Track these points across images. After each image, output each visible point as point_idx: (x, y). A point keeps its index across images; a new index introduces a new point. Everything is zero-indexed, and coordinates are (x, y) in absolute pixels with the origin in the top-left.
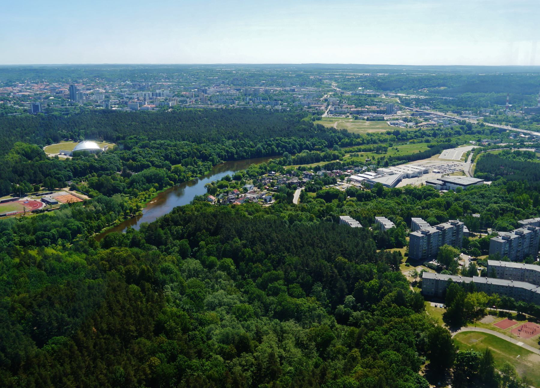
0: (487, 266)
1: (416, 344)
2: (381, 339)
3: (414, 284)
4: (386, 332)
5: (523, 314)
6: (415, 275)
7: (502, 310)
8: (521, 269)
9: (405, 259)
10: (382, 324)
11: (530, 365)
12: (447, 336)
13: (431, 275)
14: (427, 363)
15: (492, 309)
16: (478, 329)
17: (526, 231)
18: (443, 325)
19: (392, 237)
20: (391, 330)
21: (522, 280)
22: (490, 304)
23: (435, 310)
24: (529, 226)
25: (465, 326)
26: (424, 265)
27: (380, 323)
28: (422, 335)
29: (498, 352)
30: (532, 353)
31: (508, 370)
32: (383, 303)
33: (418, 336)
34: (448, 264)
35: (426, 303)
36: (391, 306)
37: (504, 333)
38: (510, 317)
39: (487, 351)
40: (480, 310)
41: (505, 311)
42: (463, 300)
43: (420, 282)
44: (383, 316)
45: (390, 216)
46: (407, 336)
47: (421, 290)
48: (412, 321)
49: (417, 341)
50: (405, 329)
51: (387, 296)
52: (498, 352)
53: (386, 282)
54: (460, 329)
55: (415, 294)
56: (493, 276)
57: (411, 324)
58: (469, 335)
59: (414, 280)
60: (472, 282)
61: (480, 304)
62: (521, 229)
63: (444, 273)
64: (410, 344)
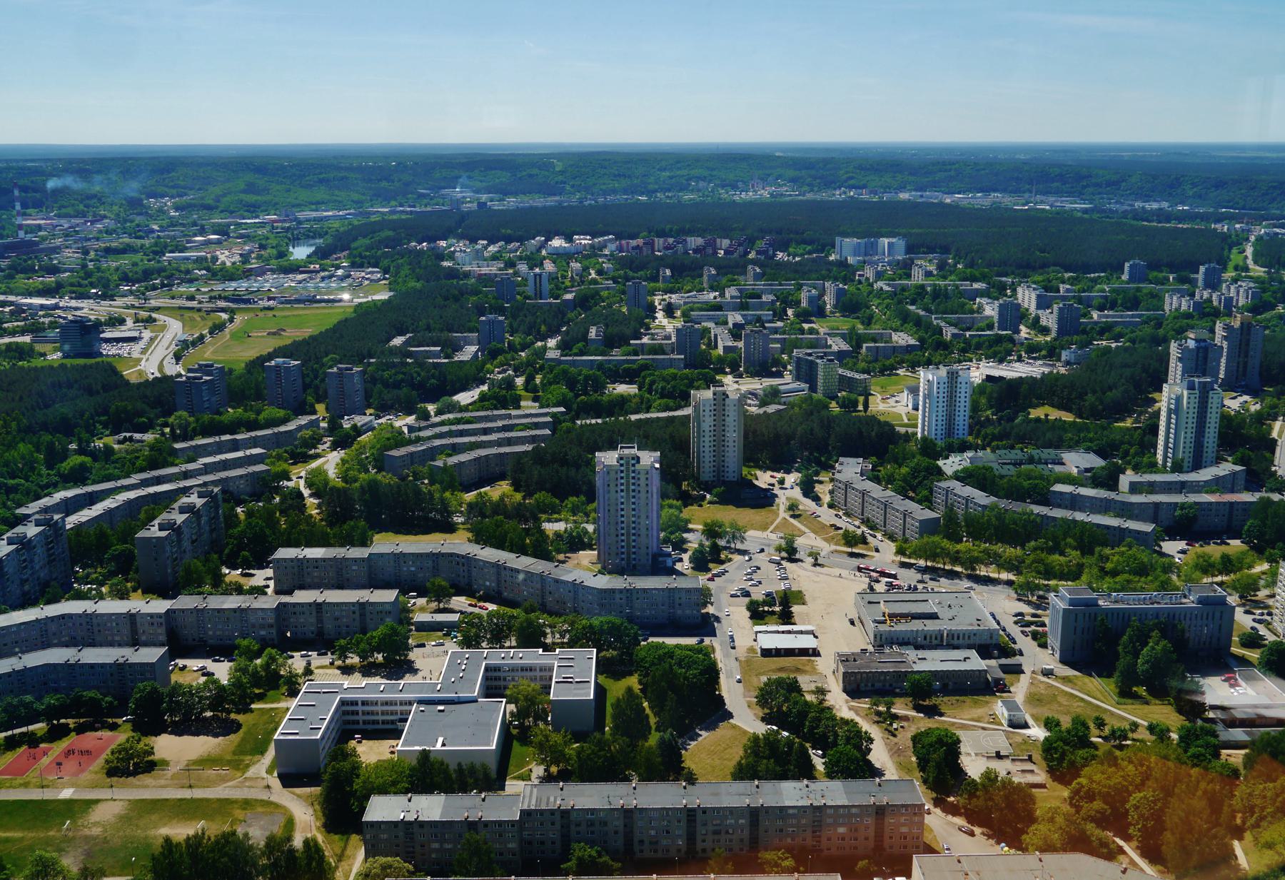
5: (62, 721)
7: (10, 733)
11: (96, 831)
17: (31, 531)
21: (45, 645)
24: (37, 516)
29: (17, 834)
30: (97, 801)
37: (26, 785)
41: (17, 731)
52: (17, 834)
62: (19, 529)
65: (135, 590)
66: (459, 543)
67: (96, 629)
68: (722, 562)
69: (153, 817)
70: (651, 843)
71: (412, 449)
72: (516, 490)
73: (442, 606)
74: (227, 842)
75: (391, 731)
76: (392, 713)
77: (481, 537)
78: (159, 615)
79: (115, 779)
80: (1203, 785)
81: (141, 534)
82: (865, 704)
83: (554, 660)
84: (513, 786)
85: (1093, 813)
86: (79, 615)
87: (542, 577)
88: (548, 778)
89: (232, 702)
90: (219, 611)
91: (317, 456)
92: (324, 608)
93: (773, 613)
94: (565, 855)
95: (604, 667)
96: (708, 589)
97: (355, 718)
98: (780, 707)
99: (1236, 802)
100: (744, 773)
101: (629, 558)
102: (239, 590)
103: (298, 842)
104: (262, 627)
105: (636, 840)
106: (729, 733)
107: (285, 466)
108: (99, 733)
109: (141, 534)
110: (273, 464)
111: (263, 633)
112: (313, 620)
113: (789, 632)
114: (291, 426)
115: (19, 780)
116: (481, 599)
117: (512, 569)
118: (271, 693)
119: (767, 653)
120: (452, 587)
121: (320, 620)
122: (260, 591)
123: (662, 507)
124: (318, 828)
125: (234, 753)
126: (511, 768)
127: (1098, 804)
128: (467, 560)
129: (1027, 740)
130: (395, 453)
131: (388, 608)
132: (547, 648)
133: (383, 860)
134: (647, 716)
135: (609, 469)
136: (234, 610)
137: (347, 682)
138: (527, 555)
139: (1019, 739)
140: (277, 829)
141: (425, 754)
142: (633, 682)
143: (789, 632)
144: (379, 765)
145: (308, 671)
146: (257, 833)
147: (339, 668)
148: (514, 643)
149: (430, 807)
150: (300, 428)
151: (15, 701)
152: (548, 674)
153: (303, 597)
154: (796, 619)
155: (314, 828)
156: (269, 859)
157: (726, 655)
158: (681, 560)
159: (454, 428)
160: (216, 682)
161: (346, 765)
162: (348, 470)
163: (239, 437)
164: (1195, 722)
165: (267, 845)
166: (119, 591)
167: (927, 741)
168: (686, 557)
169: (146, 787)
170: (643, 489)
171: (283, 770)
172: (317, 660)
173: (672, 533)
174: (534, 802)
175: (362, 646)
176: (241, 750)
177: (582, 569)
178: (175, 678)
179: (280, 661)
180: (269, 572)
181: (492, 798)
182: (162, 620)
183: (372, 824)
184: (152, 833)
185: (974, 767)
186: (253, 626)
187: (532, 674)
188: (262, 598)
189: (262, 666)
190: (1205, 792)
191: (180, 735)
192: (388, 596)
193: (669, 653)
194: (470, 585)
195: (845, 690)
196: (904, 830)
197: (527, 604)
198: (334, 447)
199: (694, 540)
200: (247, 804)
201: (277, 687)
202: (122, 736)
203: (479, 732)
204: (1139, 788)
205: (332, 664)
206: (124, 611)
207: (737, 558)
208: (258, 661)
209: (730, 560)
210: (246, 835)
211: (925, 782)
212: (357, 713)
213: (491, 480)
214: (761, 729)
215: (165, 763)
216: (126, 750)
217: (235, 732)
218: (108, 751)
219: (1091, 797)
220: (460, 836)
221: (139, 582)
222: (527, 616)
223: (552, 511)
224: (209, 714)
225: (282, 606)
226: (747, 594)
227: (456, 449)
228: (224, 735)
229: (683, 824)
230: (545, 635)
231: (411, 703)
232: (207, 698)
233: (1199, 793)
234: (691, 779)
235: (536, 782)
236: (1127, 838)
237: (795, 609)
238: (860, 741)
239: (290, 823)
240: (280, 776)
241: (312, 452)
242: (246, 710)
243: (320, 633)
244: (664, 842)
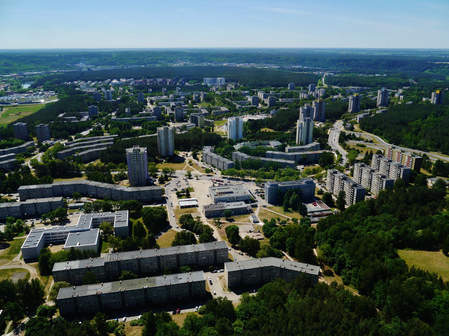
66: (83, 181)
68: (169, 181)
70: (147, 268)
71: (67, 151)
72: (102, 162)
73: (78, 201)
74: (5, 283)
76: (62, 236)
77: (90, 178)
80: (305, 235)
82: (212, 220)
83: (114, 215)
84: (103, 255)
85: (276, 245)
87: (110, 189)
88: (114, 252)
89: (6, 238)
91: (34, 155)
92: (37, 205)
93: (184, 195)
94: (120, 275)
95: (130, 216)
96: (164, 189)
98: (186, 223)
99: (315, 238)
100: (175, 244)
101: (139, 181)
102: (7, 201)
104: (16, 212)
105: (142, 268)
106: (172, 232)
107: (23, 159)
110: (18, 158)
111: (16, 214)
112: (34, 209)
113: (189, 200)
114: (24, 145)
116: (91, 198)
117: (100, 188)
118: (20, 233)
119: (182, 207)
120: (81, 194)
121: (36, 209)
122: (14, 201)
123: (149, 165)
124: (38, 275)
125: (8, 254)
126: (102, 250)
127: (277, 243)
128: (86, 186)
129: (259, 226)
130: (61, 152)
131: (59, 203)
132: (113, 211)
133: (59, 283)
134: (145, 230)
135: (130, 154)
137: (46, 228)
138: (105, 183)
139: (256, 226)
140: (23, 277)
141: (72, 248)
142: (141, 220)
143: (189, 200)
145: (33, 226)
147: (44, 223)
149: (75, 265)
150: (27, 146)
153: (29, 201)
154: (191, 196)
155: (37, 275)
157: (170, 209)
158: (156, 181)
159: (81, 143)
161: (46, 254)
162: (45, 159)
163: (5, 150)
164: (304, 217)
165: (19, 283)
167: (229, 229)
168: (157, 180)
170: (142, 160)
171: (26, 258)
173: (152, 173)
174: (109, 259)
175: (51, 216)
176: (10, 253)
177: (124, 186)
180: (18, 194)
181: (95, 260)
185: (243, 235)
186: (12, 212)
187: (108, 220)
189: (16, 225)
190: (306, 237)
192: (59, 199)
193: (151, 210)
194: (87, 193)
195: (206, 217)
196: (223, 256)
197: (105, 198)
198: (40, 151)
199: (160, 174)
200: (13, 270)
201: (22, 232)
203: (91, 239)
204: (288, 237)
205: (41, 222)
207: (173, 179)
208: (15, 224)
209: (171, 180)
210: (11, 280)
211: (229, 241)
213: (94, 160)
214: (180, 230)
217: (8, 247)
219: (275, 240)
220: (85, 272)
222: (106, 201)
223: (114, 168)
225: (22, 205)
226: (176, 190)
227: (82, 150)
228: (4, 249)
229: (156, 261)
230: (112, 207)
231: (68, 233)
233: (304, 237)
234: (158, 248)
235: (111, 253)
236: (285, 252)
237: (191, 193)
238: (210, 231)
239: (29, 275)
240: (25, 260)
241: (32, 153)
243: (37, 213)
244: (151, 267)
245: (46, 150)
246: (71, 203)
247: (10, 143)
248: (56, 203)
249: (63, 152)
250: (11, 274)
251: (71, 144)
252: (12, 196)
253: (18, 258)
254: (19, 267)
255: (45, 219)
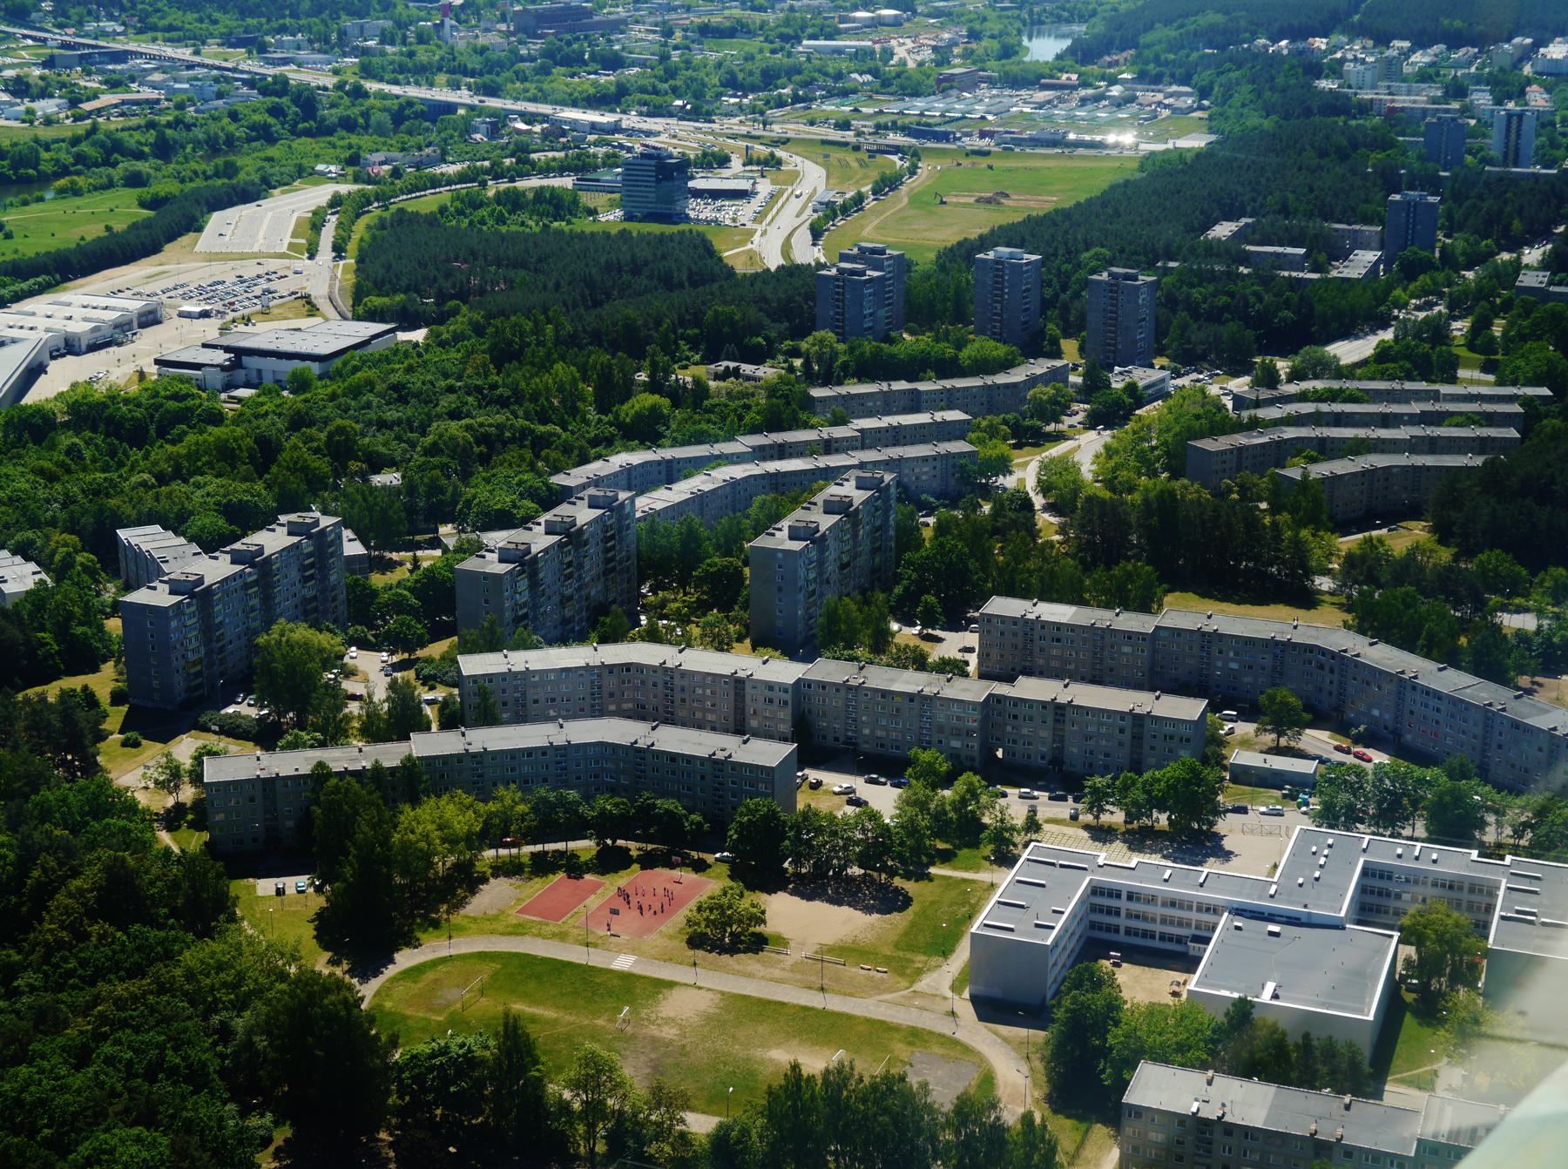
0: (458, 681)
1: (222, 1072)
2: (63, 1089)
3: (173, 819)
4: (81, 1057)
5: (620, 842)
6: (172, 778)
7: (539, 848)
8: (587, 668)
9: (115, 717)
10: (59, 1025)
11: (669, 1033)
12: (345, 1002)
13: (239, 764)
14: (282, 1135)
15: (503, 852)
16: (463, 946)
17: (583, 515)
18: (321, 964)
19: (43, 629)
20: (105, 1037)
21: (598, 712)
22: (492, 834)
23: (280, 909)
24: (592, 491)
25: (412, 942)
26: (205, 729)
27: (47, 1021)
28: (239, 1024)
29: (550, 1014)
30: (671, 985)
31: (595, 1075)
32: (49, 928)
33: (225, 1033)
34: (301, 702)
35: (237, 887)
36: (87, 936)
37: (562, 937)
38: (574, 867)
39: (506, 1025)
40: (456, 866)
41: (550, 847)
42: (385, 843)
43: (198, 805)
44: (60, 988)
45: (18, 537)
46: (175, 1049)
47: (206, 836)
48: (190, 976)
49: (222, 1056)
50: (166, 1020)
51: (61, 898)
52: (550, 1014)
53: (48, 834)
54: (392, 961)
55: (185, 859)
56: (488, 718)
57: (185, 994)
58: (430, 975)
59: (170, 802)
60: (409, 758)
61: (452, 841)
62: (564, 510)
63: (294, 745)
64: (196, 1078)
65: (740, 639)
66: (1325, 629)
67: (678, 696)
69: (763, 1029)
71: (1241, 440)
72: (1443, 541)
73: (1283, 742)
75: (1177, 954)
76: (1180, 924)
77: (1372, 622)
78: (784, 688)
79: (700, 953)
81: (762, 541)
86: (654, 669)
87: (1488, 716)
89: (900, 857)
90: (885, 694)
91: (1059, 437)
92: (1069, 713)
97: (1112, 920)
102: (919, 662)
103: (1010, 1115)
104: (957, 733)
107: (1003, 448)
108: (676, 873)
109: (762, 541)
110: (981, 442)
111: (955, 744)
112: (1045, 734)
114: (1017, 376)
115: (552, 927)
116: (1357, 740)
117: (1428, 692)
118: (964, 852)
120: (1307, 708)
121: (1059, 738)
122: (954, 668)
124: (1037, 1101)
125: (897, 946)
126: (1397, 1062)
128: (1340, 663)
130: (1208, 444)
131: (1189, 733)
136: (911, 697)
137: (1104, 854)
138: (1459, 668)
144: (1153, 1011)
145: (1033, 825)
146: (942, 1088)
147: (1086, 827)
148: (1421, 831)
149: (1250, 1103)
150: (1033, 381)
151: (552, 796)
152: (1484, 900)
153: (1030, 688)
155: (1029, 1100)
156: (957, 1133)
159: (1325, 407)
160: (874, 816)
161: (1098, 1000)
162: (1115, 469)
163: (923, 386)
166: (715, 636)
169: (750, 975)
171: (981, 990)
172: (1048, 808)
178: (803, 800)
179: (984, 799)
180: (972, 639)
182: (788, 697)
183: (1138, 1112)
184: (758, 1053)
186: (941, 729)
187: (1454, 894)
188: (959, 682)
191: (810, 898)
192: (1189, 709)
194: (1339, 709)
198: (1092, 423)
200: (916, 1036)
201: (974, 844)
202: (710, 884)
205: (1074, 818)
206: (727, 671)
208: (947, 793)
210: (924, 1086)
212: (1118, 913)
213: (1393, 516)
215: (782, 942)
216: (721, 907)
217: (902, 909)
218: (693, 904)
221: (747, 626)
223: (1514, 592)
224: (855, 871)
227: (1326, 449)
230: (1482, 825)
232: (857, 843)
239: (988, 1080)
240: (976, 1000)
241: (1051, 428)
242: (922, 876)
243: (1057, 760)
245: (1126, 418)
246: (1246, 744)
247: (950, 351)
248: (1173, 733)
249: (1222, 443)
250: (905, 1056)
251: (1271, 402)
252: (939, 640)
253: (944, 977)
254: (945, 1028)
255: (1097, 807)
